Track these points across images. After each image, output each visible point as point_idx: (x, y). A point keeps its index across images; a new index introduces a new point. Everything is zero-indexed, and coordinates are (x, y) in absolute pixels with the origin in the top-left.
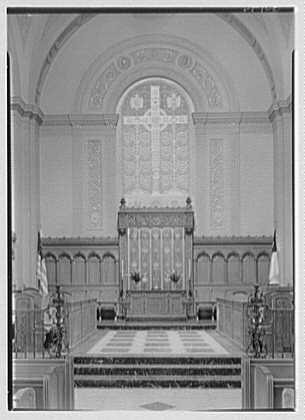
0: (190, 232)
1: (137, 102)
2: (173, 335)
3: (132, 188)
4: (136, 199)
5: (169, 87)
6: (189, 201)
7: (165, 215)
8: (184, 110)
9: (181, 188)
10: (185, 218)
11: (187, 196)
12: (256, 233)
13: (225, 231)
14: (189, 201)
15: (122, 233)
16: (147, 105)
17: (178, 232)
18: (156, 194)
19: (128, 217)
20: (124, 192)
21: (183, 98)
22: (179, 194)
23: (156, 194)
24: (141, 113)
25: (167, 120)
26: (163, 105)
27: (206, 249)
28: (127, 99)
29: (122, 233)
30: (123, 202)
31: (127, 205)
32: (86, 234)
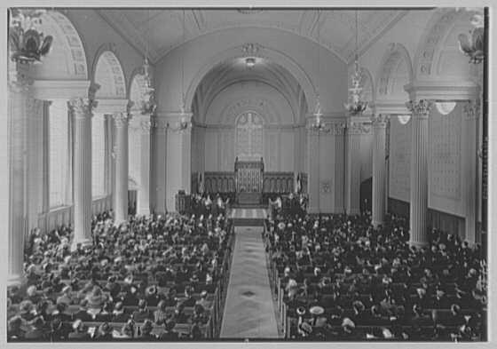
0: (262, 170)
2: (254, 211)
4: (242, 158)
7: (253, 164)
8: (261, 122)
9: (259, 153)
10: (261, 165)
12: (287, 171)
13: (276, 170)
15: (236, 170)
16: (247, 121)
17: (259, 170)
19: (237, 165)
20: (237, 154)
24: (244, 124)
25: (254, 126)
26: (253, 121)
27: (268, 176)
29: (236, 170)
30: (237, 159)
31: (239, 160)
32: (222, 170)
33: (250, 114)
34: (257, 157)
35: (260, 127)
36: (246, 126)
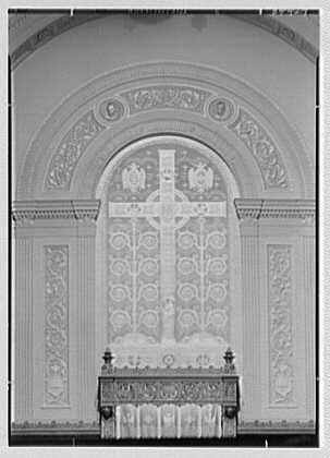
1: (134, 178)
3: (124, 332)
4: (132, 352)
5: (193, 153)
6: (229, 357)
7: (188, 384)
8: (220, 189)
9: (212, 331)
11: (225, 347)
14: (229, 357)
16: (153, 183)
18: (168, 343)
20: (111, 338)
21: (216, 172)
22: (211, 342)
23: (168, 343)
24: (141, 196)
25: (188, 209)
26: (181, 183)
28: (117, 172)
30: (108, 358)
33: (171, 153)
34: (202, 352)
35: (218, 209)
36: (149, 209)
